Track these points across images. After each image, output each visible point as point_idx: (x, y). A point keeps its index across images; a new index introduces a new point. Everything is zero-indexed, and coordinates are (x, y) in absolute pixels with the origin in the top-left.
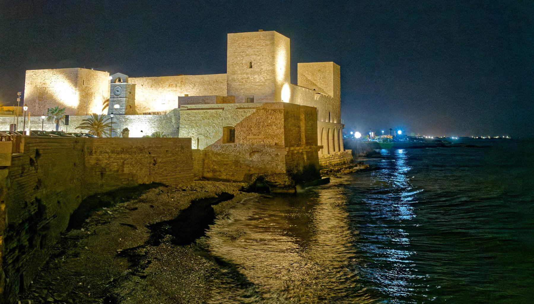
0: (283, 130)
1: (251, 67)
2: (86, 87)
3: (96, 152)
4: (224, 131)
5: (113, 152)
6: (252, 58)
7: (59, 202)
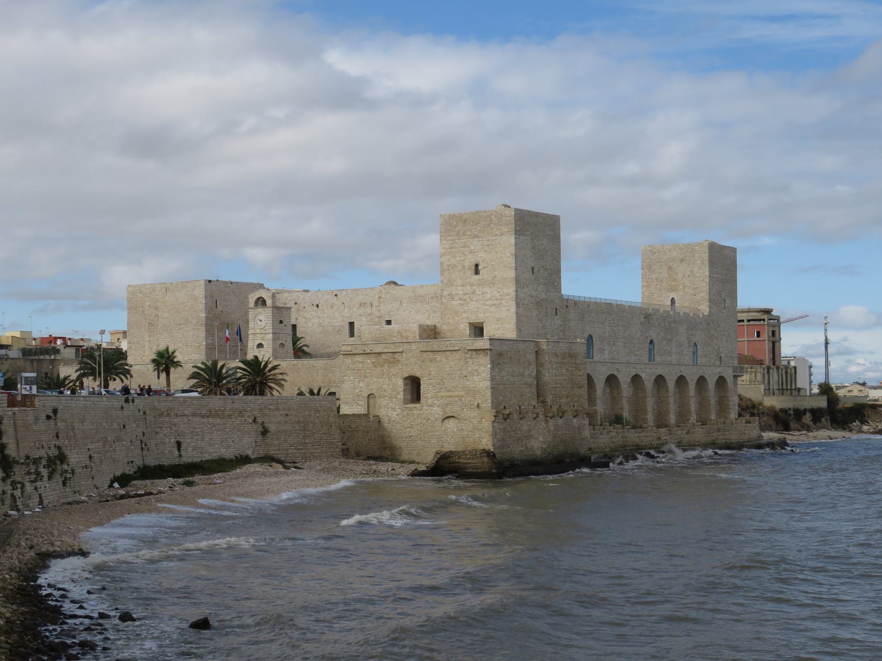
0: (488, 383)
1: (477, 272)
3: (168, 415)
4: (405, 385)
6: (480, 257)
7: (90, 457)
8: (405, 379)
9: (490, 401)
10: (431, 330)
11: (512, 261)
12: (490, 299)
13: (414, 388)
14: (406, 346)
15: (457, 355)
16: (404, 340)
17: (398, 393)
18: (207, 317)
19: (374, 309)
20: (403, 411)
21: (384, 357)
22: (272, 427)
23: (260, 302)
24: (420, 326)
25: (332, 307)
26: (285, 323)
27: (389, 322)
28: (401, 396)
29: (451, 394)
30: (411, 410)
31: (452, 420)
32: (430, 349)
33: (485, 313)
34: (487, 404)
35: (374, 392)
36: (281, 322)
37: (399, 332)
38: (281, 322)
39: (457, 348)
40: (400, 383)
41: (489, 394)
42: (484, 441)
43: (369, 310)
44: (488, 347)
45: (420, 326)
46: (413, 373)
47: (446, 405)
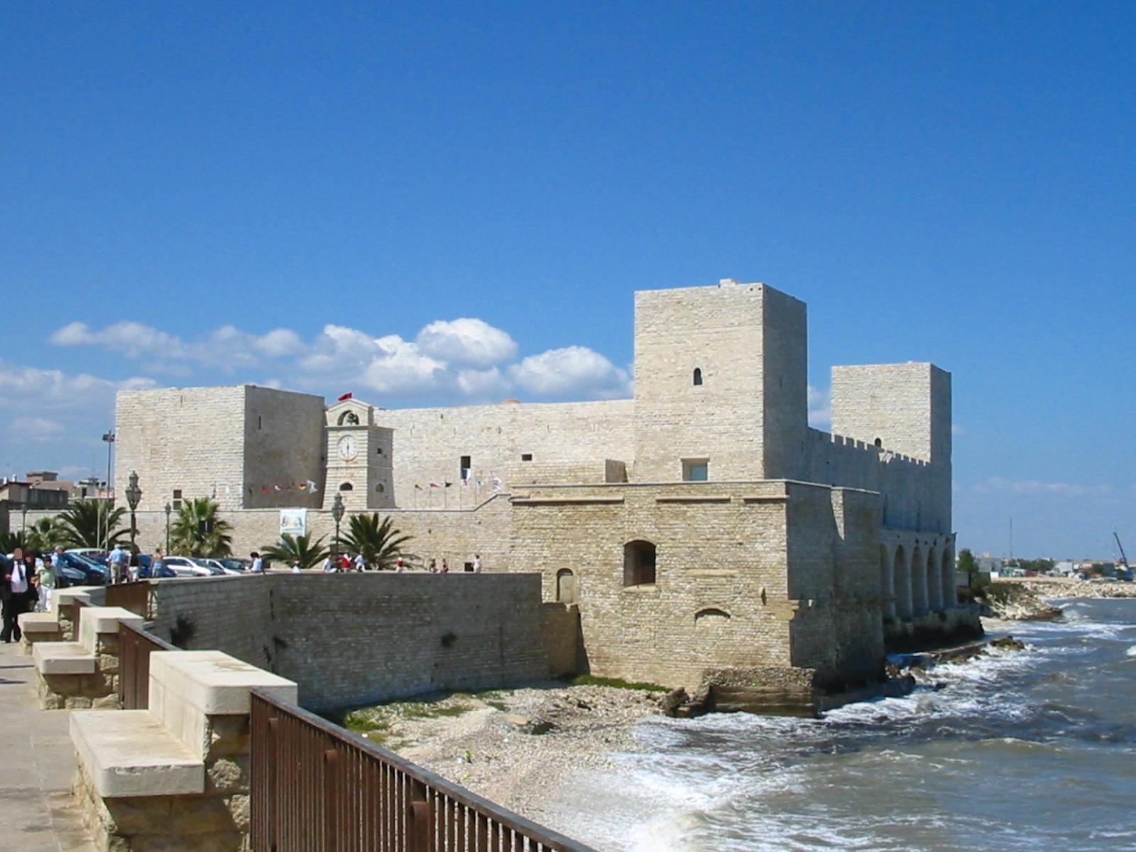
0: (785, 555)
2: (267, 435)
5: (343, 608)
8: (626, 546)
9: (786, 585)
10: (620, 468)
11: (758, 367)
13: (642, 561)
16: (580, 483)
17: (614, 567)
18: (245, 443)
19: (503, 437)
20: (623, 598)
21: (589, 507)
22: (458, 630)
23: (346, 418)
24: (608, 462)
25: (434, 433)
26: (384, 452)
27: (527, 458)
28: (619, 573)
29: (712, 572)
30: (637, 596)
31: (711, 618)
34: (780, 588)
35: (569, 566)
36: (380, 451)
37: (570, 471)
38: (380, 451)
39: (725, 496)
40: (618, 555)
41: (785, 572)
42: (774, 652)
43: (495, 437)
44: (785, 496)
45: (608, 462)
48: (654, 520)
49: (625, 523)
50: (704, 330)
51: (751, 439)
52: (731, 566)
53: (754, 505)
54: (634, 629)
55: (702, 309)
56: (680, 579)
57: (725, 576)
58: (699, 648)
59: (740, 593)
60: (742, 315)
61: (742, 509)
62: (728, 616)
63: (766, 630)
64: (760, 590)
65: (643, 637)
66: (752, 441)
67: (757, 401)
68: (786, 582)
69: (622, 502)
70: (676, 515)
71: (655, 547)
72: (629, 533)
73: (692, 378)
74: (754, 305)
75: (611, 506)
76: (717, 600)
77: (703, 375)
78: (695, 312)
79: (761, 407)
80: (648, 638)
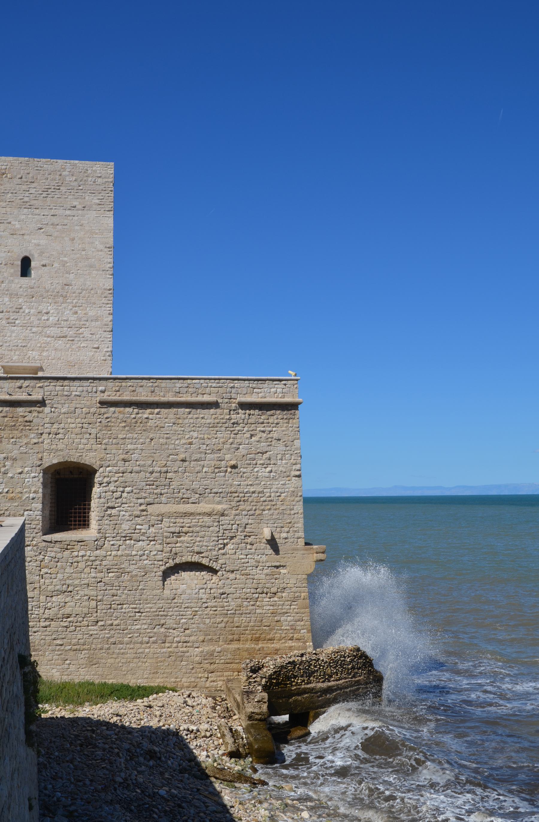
8: (46, 471)
11: (108, 260)
12: (57, 324)
14: (51, 388)
15: (208, 414)
30: (67, 547)
31: (185, 575)
32: (127, 397)
33: (42, 349)
39: (206, 398)
46: (74, 457)
47: (179, 534)
48: (94, 431)
49: (45, 436)
50: (37, 211)
51: (96, 346)
52: (217, 499)
53: (252, 412)
54: (61, 598)
55: (33, 185)
56: (139, 520)
57: (209, 515)
58: (170, 622)
59: (232, 538)
60: (87, 198)
61: (233, 416)
62: (214, 571)
63: (274, 590)
64: (267, 533)
65: (78, 610)
66: (98, 348)
67: (104, 300)
68: (302, 521)
69: (42, 403)
70: (131, 426)
71: (95, 471)
72: (50, 451)
73: (19, 269)
74: (102, 187)
75: (20, 410)
76: (196, 549)
77: (33, 264)
78: (24, 187)
79: (109, 308)
80: (85, 610)
